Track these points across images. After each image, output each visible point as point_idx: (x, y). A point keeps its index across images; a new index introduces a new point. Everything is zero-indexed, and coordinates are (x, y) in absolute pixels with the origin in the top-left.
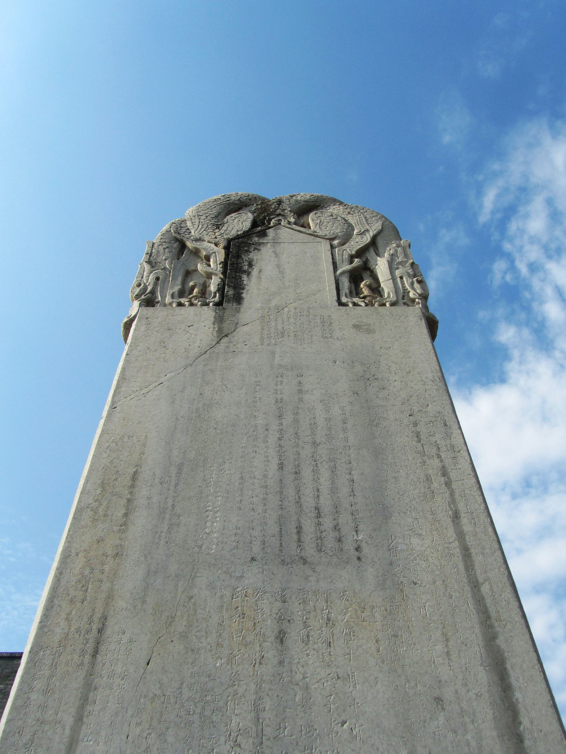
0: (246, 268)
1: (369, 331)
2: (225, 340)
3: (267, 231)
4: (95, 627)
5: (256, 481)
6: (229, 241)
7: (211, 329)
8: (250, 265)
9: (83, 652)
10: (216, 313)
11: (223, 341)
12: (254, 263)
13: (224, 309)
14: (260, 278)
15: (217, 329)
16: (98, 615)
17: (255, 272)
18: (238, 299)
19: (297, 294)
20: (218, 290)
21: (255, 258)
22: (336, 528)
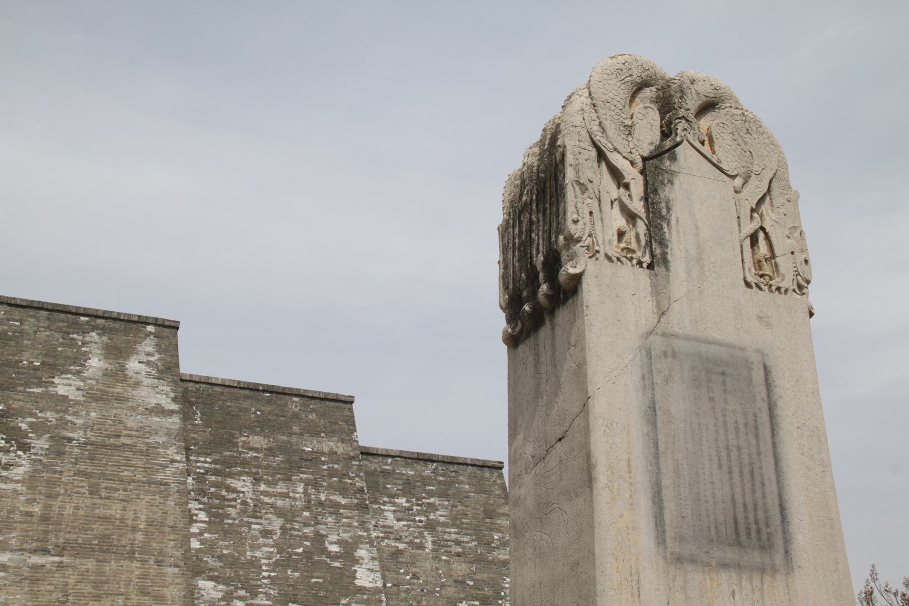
0: (664, 211)
1: (768, 325)
2: (663, 319)
3: (676, 149)
4: (635, 578)
5: (706, 477)
6: (645, 159)
7: (651, 303)
8: (669, 209)
9: (633, 594)
10: (651, 280)
11: (662, 320)
12: (670, 205)
13: (656, 275)
14: (678, 231)
15: (655, 304)
16: (634, 571)
17: (673, 222)
18: (665, 262)
19: (712, 263)
20: (646, 244)
21: (671, 196)
22: (756, 523)
